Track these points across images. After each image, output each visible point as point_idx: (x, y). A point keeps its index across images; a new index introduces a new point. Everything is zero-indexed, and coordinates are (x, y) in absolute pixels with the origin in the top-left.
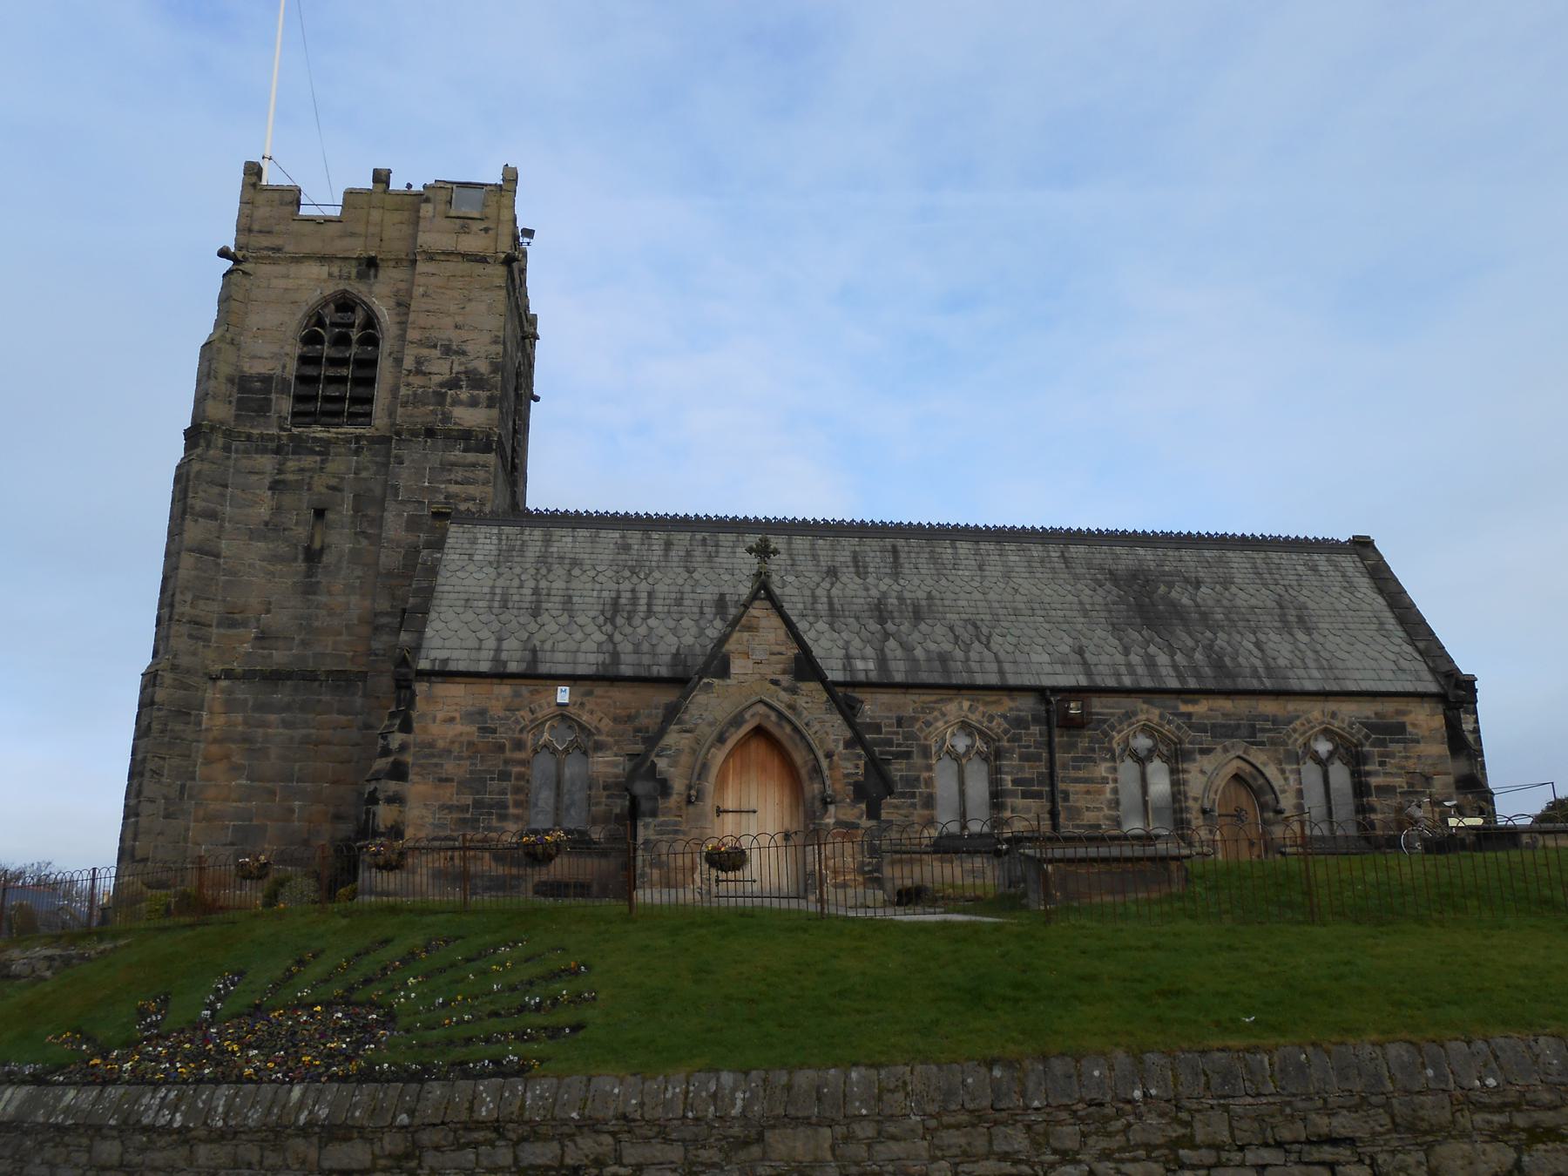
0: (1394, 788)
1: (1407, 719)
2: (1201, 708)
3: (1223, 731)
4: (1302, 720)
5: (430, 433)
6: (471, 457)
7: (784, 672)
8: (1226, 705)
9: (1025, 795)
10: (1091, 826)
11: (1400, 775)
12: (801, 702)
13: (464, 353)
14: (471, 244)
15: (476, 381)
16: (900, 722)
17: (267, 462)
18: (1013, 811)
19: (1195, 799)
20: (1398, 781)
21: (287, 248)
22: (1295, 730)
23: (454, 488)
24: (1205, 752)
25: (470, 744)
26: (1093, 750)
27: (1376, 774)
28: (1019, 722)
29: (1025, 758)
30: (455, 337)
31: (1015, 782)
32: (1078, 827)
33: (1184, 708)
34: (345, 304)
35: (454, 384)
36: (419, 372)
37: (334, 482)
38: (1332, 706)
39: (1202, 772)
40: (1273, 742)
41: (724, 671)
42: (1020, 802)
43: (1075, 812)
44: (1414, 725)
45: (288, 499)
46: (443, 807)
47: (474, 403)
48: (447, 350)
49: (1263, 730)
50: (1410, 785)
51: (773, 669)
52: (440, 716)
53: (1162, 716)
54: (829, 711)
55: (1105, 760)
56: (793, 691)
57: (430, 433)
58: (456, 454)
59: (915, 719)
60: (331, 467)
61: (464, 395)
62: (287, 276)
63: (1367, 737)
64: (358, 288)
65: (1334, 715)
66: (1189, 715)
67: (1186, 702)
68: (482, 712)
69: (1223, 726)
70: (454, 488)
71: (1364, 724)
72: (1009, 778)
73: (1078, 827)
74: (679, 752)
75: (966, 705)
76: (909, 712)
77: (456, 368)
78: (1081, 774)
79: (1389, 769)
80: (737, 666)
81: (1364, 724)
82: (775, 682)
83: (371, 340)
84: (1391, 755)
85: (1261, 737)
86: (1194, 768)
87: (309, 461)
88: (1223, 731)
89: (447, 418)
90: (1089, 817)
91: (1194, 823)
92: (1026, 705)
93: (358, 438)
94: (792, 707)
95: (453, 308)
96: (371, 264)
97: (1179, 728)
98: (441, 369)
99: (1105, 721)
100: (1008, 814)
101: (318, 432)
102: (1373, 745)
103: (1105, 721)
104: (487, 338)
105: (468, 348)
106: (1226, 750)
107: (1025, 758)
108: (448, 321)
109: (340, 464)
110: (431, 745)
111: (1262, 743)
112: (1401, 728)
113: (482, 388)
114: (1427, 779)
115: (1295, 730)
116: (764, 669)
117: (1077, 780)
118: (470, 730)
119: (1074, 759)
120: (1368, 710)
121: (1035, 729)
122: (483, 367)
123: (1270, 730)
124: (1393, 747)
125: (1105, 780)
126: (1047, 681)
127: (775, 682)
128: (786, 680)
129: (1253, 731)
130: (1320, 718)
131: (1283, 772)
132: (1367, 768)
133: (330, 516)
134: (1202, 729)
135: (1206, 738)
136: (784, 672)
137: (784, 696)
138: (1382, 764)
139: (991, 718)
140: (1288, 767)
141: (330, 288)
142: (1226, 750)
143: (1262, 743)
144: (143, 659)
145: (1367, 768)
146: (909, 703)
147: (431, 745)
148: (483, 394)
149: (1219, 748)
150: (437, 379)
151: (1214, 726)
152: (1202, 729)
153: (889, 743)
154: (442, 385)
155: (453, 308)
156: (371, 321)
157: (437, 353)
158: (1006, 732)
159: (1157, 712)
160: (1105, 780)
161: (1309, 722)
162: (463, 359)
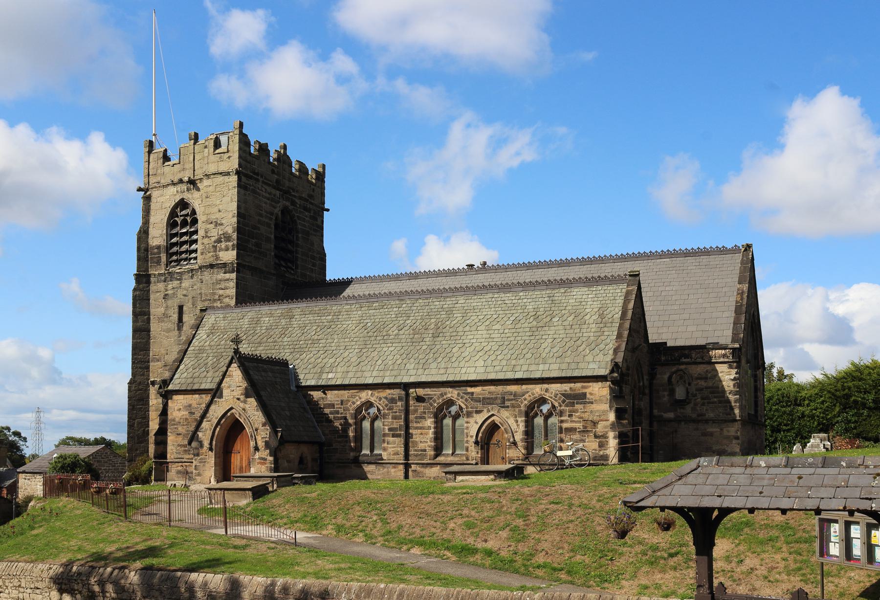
0: (575, 429)
1: (587, 391)
2: (477, 390)
3: (487, 401)
4: (530, 393)
5: (212, 266)
6: (227, 276)
7: (242, 394)
8: (492, 388)
9: (393, 436)
10: (422, 450)
11: (580, 422)
12: (247, 406)
13: (222, 224)
14: (223, 167)
15: (228, 238)
16: (342, 402)
17: (161, 286)
18: (388, 443)
19: (472, 437)
20: (579, 426)
21: (162, 181)
22: (525, 399)
23: (221, 292)
24: (478, 412)
25: (186, 419)
26: (425, 413)
27: (566, 421)
28: (393, 401)
29: (394, 418)
30: (218, 215)
31: (390, 430)
32: (416, 450)
33: (470, 390)
34: (183, 204)
35: (219, 241)
36: (207, 236)
37: (185, 292)
38: (546, 386)
39: (476, 423)
40: (513, 406)
41: (221, 397)
42: (391, 439)
43: (416, 443)
44: (591, 394)
45: (170, 302)
46: (179, 445)
47: (227, 249)
48: (217, 224)
49: (509, 400)
50: (585, 427)
51: (238, 392)
52: (176, 408)
53: (458, 395)
54: (257, 410)
55: (430, 418)
56: (245, 402)
57: (212, 266)
58: (222, 276)
59: (349, 401)
60: (183, 285)
61: (223, 245)
62: (162, 195)
63: (564, 402)
64: (187, 196)
65: (547, 390)
66: (472, 393)
67: (471, 386)
68: (190, 406)
69: (488, 398)
70: (221, 292)
71: (563, 395)
72: (387, 428)
73: (416, 450)
74: (206, 430)
75: (370, 392)
76: (345, 398)
77: (221, 232)
78: (418, 425)
79: (574, 418)
80: (225, 392)
81: (563, 395)
82: (238, 399)
83: (195, 221)
84: (576, 411)
85: (507, 403)
86: (471, 420)
87: (176, 283)
88: (487, 401)
89: (217, 258)
90: (421, 446)
91: (470, 448)
92: (396, 393)
93: (192, 270)
94: (244, 409)
95: (218, 202)
96: (192, 182)
97: (466, 400)
98: (215, 233)
99: (431, 398)
100: (386, 445)
101: (177, 270)
102: (567, 406)
103: (431, 398)
104: (231, 215)
105: (223, 222)
106: (489, 411)
107: (394, 418)
108: (216, 209)
109: (186, 283)
110: (174, 420)
111: (508, 407)
112: (585, 394)
113: (229, 241)
114: (595, 424)
115: (525, 399)
116: (235, 393)
117: (417, 428)
118: (185, 413)
119: (416, 418)
120: (566, 387)
121: (399, 404)
122: (230, 230)
123: (512, 400)
124: (577, 406)
125: (429, 428)
126: (406, 380)
127: (238, 399)
128: (242, 398)
129: (503, 400)
130: (539, 392)
131: (517, 421)
132: (562, 418)
133: (185, 308)
134: (478, 400)
135: (479, 406)
136: (242, 394)
137: (242, 405)
138: (570, 416)
139: (380, 399)
140: (519, 419)
141: (178, 198)
142: (489, 411)
143: (508, 407)
144: (129, 377)
145: (562, 418)
146: (345, 394)
147: (174, 420)
148: (230, 244)
149: (485, 410)
150: (213, 239)
151: (484, 398)
152: (478, 400)
153: (337, 412)
154: (215, 242)
155: (218, 202)
156: (194, 212)
157: (212, 226)
158: (386, 405)
159: (456, 392)
160: (429, 428)
161: (533, 394)
162: (222, 227)
